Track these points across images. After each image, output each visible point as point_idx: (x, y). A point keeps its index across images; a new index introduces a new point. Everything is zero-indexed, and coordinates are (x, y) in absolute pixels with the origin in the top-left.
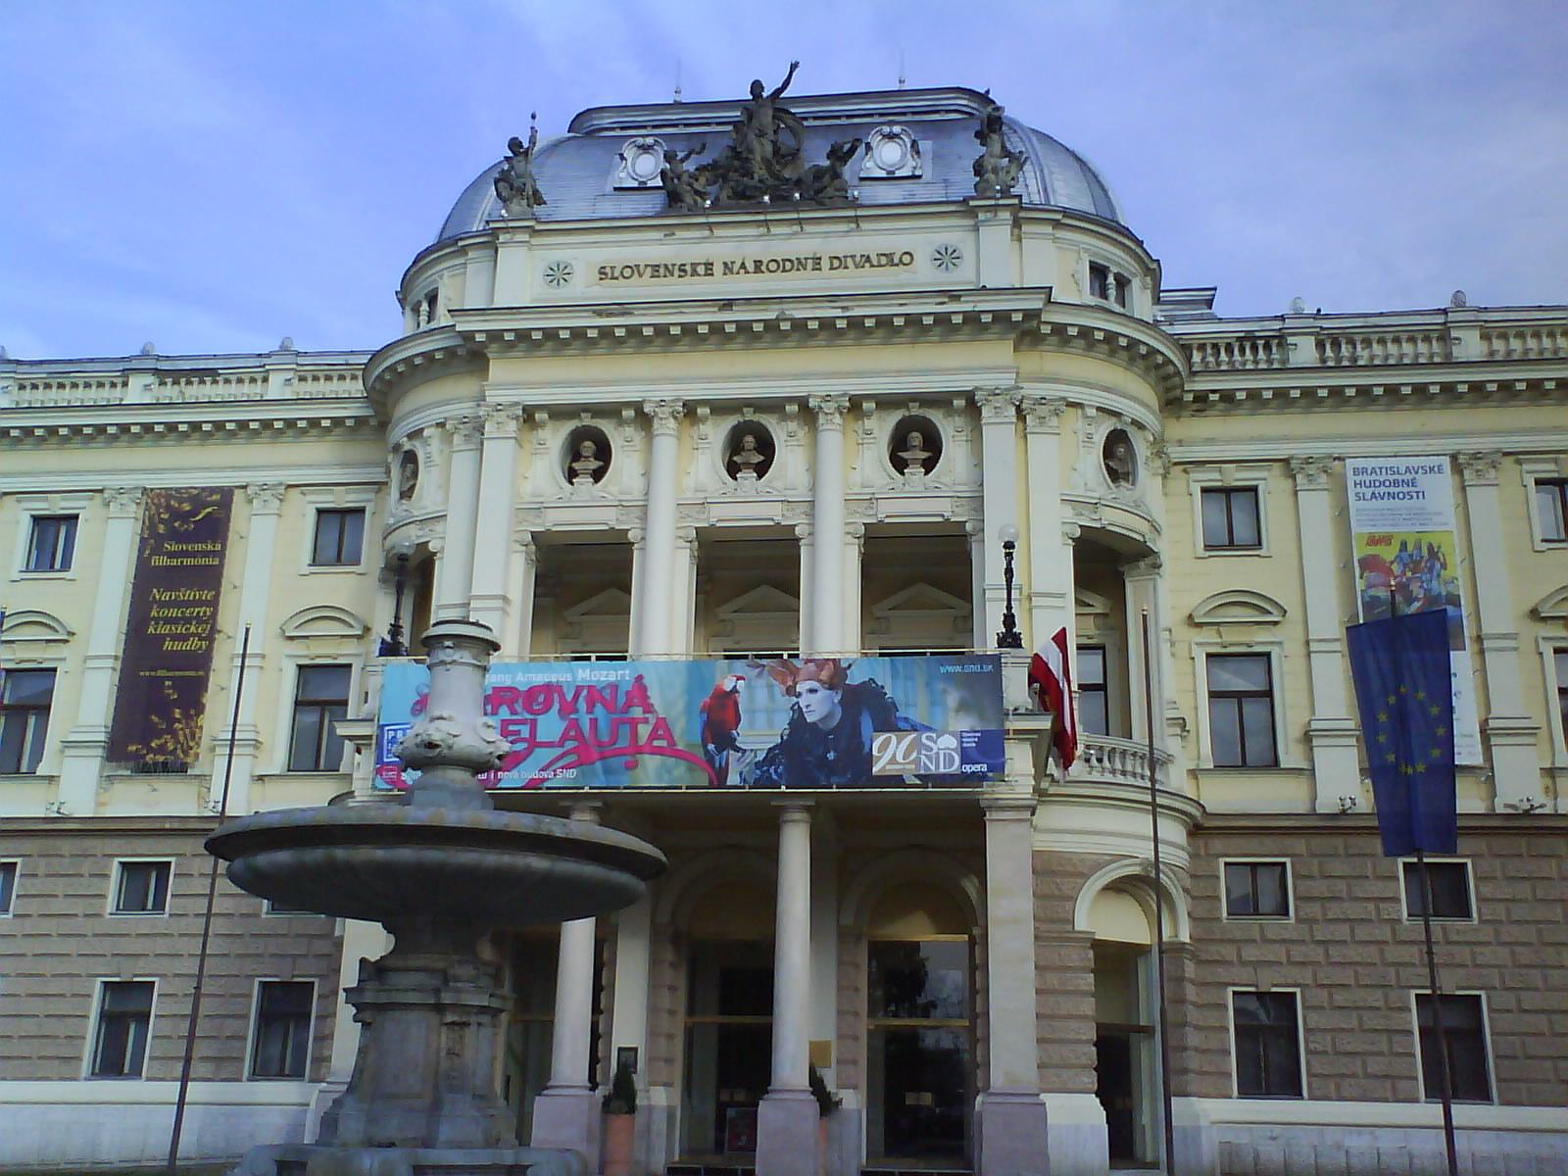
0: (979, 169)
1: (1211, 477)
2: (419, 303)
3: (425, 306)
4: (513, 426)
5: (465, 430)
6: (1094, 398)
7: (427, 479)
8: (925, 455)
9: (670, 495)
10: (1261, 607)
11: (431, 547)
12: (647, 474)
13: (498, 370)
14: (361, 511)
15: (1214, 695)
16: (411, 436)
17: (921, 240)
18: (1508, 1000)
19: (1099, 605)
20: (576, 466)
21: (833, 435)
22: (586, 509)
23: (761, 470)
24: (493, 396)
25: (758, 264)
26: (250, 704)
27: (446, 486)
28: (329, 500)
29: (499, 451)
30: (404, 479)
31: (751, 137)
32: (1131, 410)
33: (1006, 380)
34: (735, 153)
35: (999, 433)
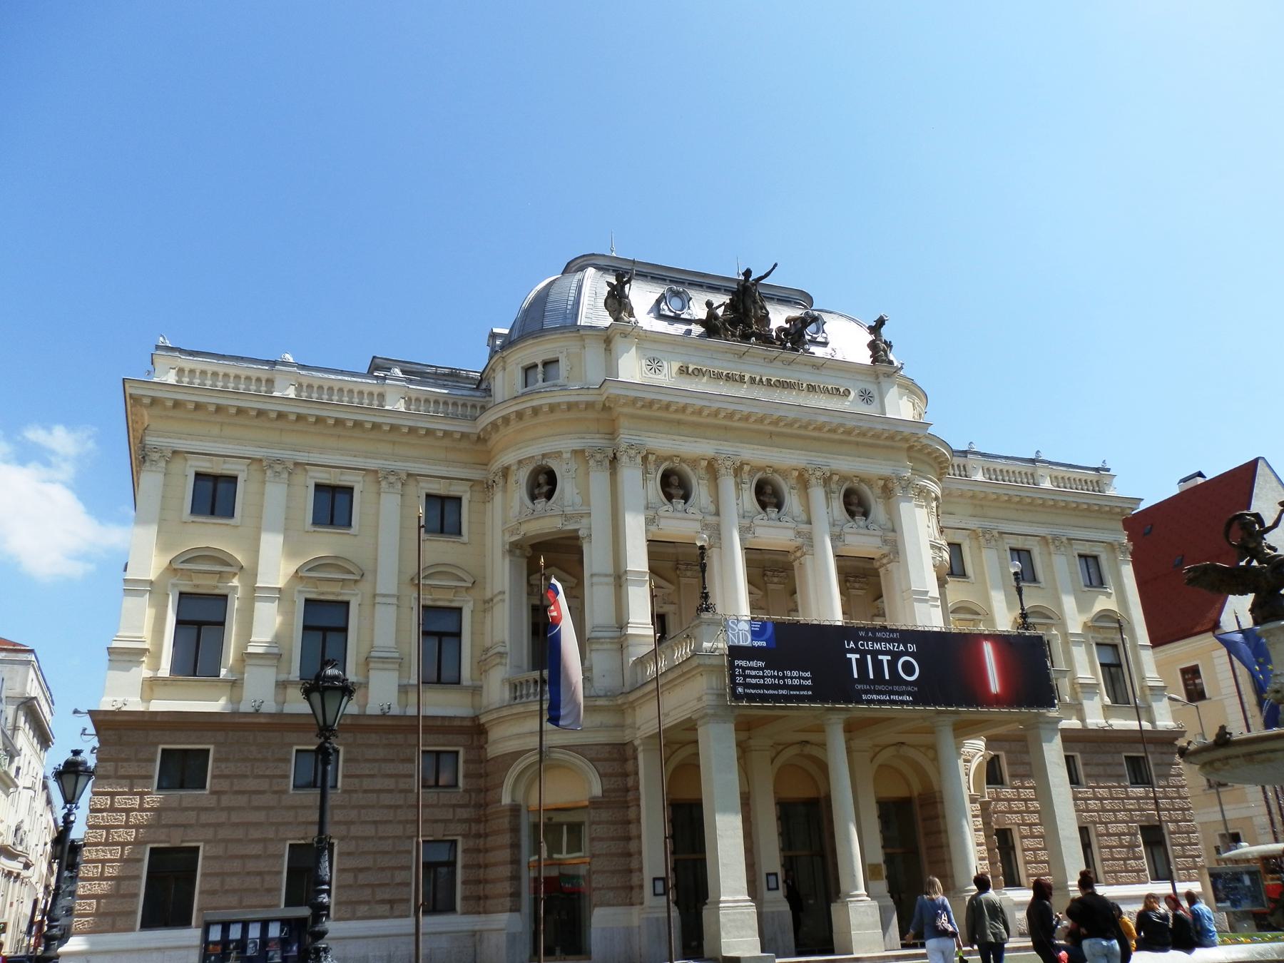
0: (873, 346)
2: (536, 366)
3: (540, 367)
4: (639, 460)
5: (598, 457)
7: (566, 487)
8: (861, 510)
11: (580, 533)
12: (716, 501)
13: (624, 423)
14: (459, 499)
16: (544, 456)
18: (1101, 828)
20: (673, 491)
25: (769, 380)
28: (439, 488)
31: (749, 302)
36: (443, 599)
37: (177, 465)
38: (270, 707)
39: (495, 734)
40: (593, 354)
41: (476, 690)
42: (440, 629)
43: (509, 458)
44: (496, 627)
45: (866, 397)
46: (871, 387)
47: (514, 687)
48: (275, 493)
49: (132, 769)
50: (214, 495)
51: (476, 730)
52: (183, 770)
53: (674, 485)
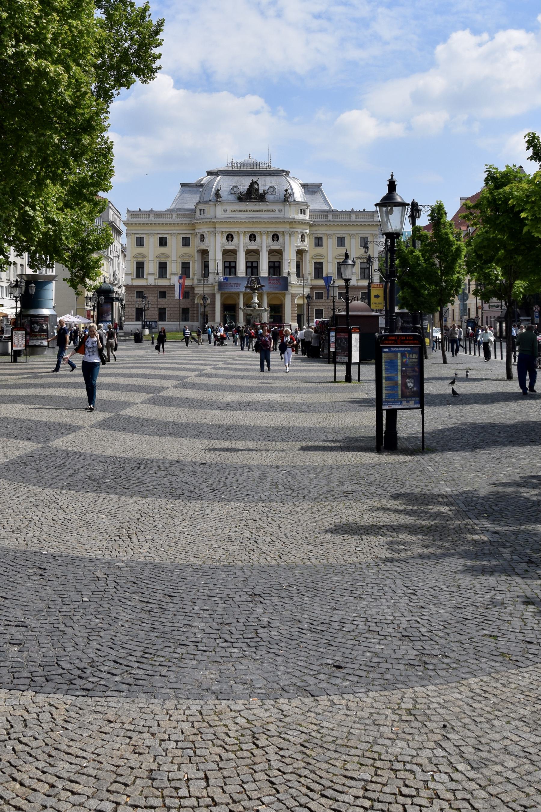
0: (285, 195)
1: (316, 236)
6: (299, 230)
9: (242, 244)
10: (322, 256)
13: (217, 226)
15: (315, 268)
17: (276, 207)
19: (300, 256)
21: (264, 237)
22: (230, 246)
23: (255, 241)
24: (217, 229)
26: (174, 268)
27: (210, 241)
29: (219, 238)
30: (201, 238)
32: (304, 231)
33: (288, 230)
34: (248, 190)
35: (287, 238)
36: (186, 260)
37: (133, 235)
38: (153, 284)
39: (196, 289)
40: (212, 208)
41: (193, 279)
42: (186, 267)
43: (197, 231)
44: (196, 268)
45: (280, 211)
46: (282, 208)
47: (198, 280)
48: (151, 240)
49: (131, 295)
50: (140, 242)
51: (192, 288)
52: (140, 295)
53: (230, 237)
